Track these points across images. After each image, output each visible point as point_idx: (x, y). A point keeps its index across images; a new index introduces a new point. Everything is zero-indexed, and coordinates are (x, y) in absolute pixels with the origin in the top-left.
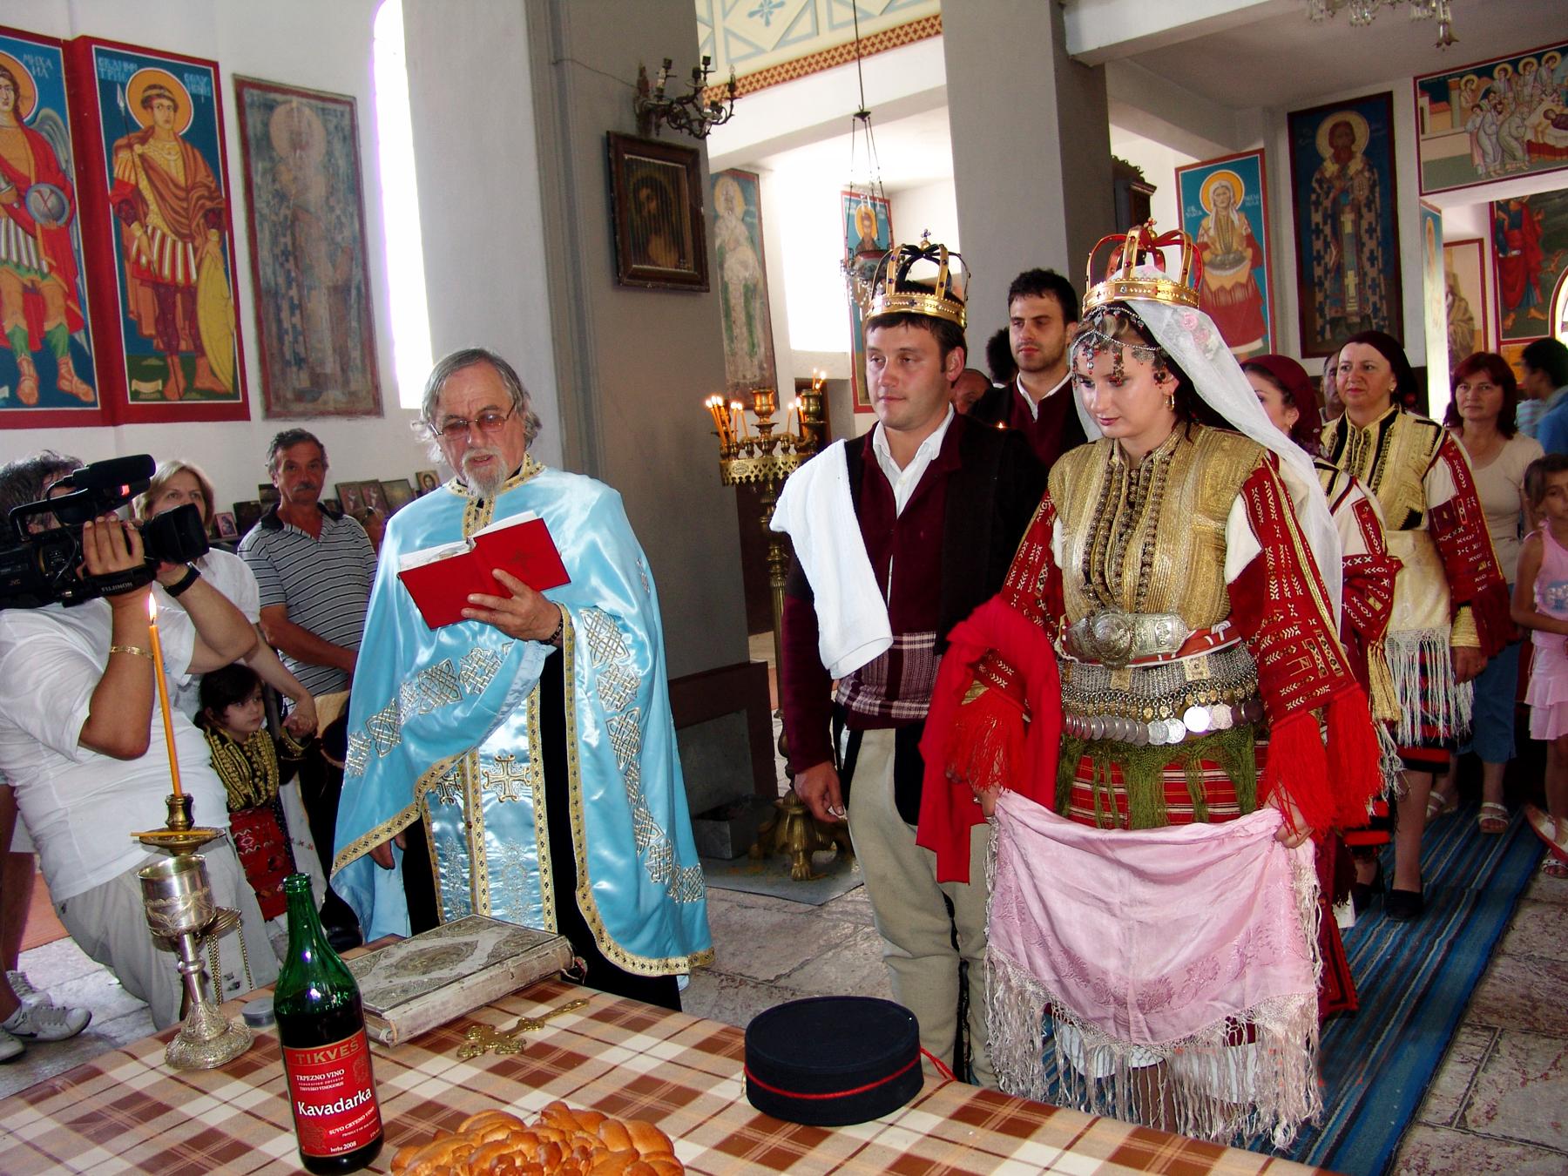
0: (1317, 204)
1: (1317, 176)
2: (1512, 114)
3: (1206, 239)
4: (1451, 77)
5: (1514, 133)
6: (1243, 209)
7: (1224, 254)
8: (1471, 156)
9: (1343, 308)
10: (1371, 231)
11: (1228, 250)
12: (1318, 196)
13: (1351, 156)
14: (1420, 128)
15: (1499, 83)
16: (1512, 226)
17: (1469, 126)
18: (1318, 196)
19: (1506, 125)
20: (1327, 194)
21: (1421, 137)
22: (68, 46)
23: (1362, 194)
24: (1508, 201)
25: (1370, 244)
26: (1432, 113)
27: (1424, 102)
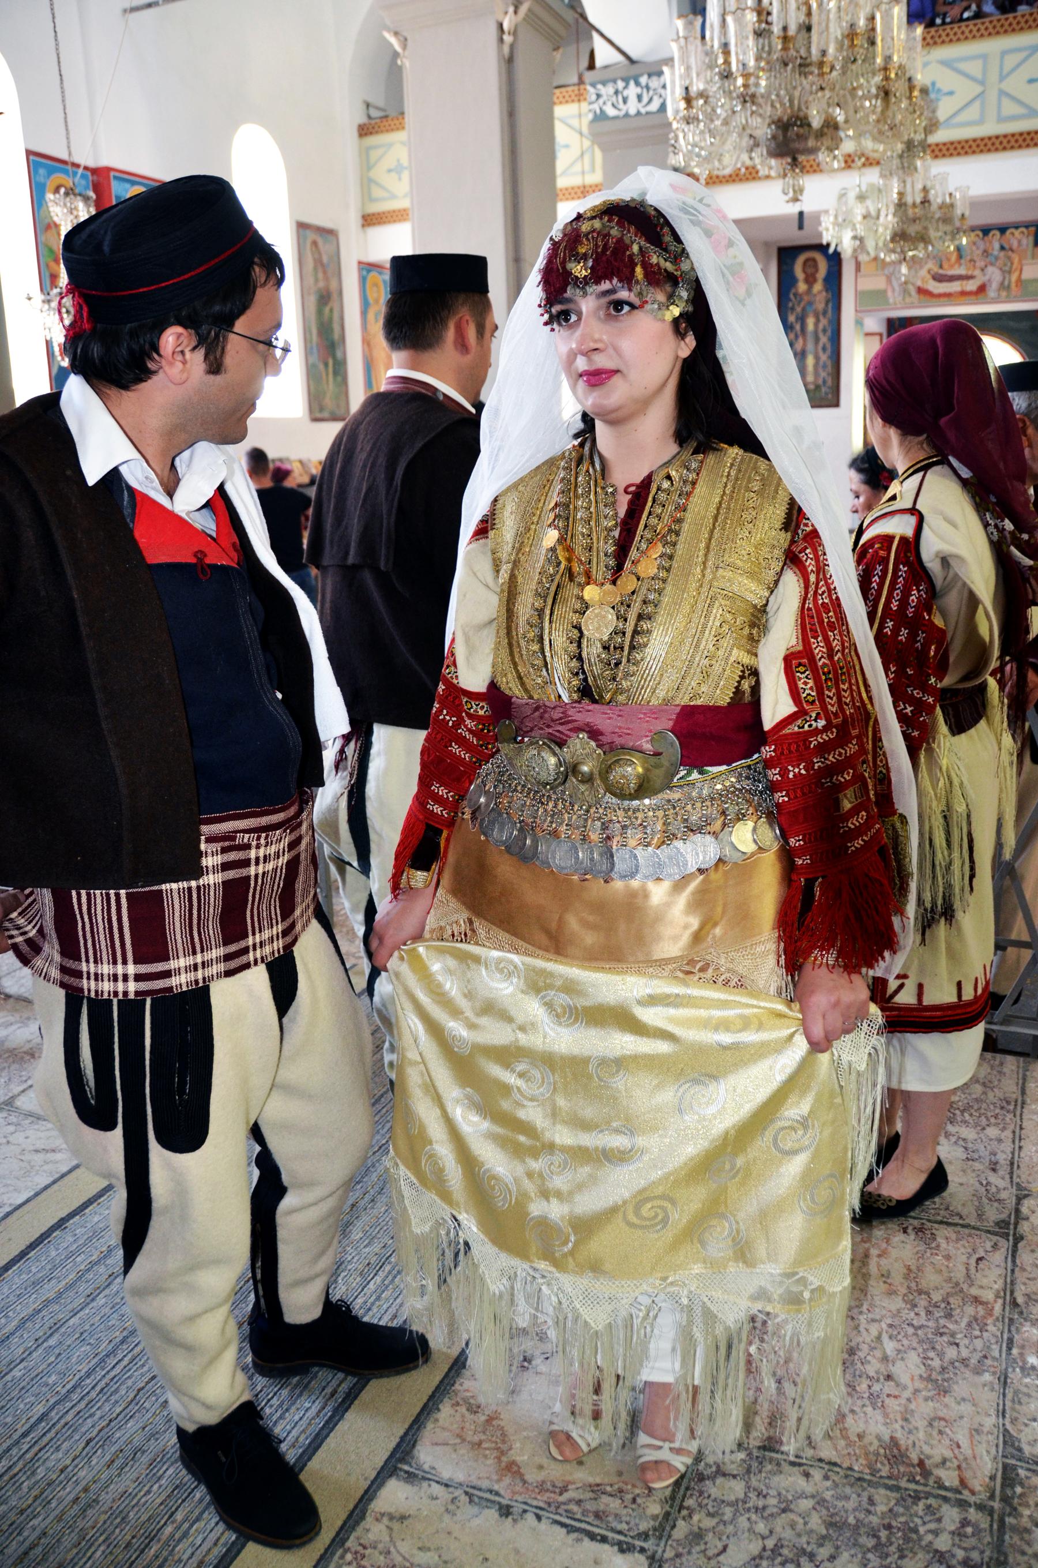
0: (793, 309)
1: (793, 291)
8: (885, 291)
10: (824, 331)
13: (815, 280)
20: (799, 303)
22: (95, 171)
23: (820, 306)
25: (824, 339)
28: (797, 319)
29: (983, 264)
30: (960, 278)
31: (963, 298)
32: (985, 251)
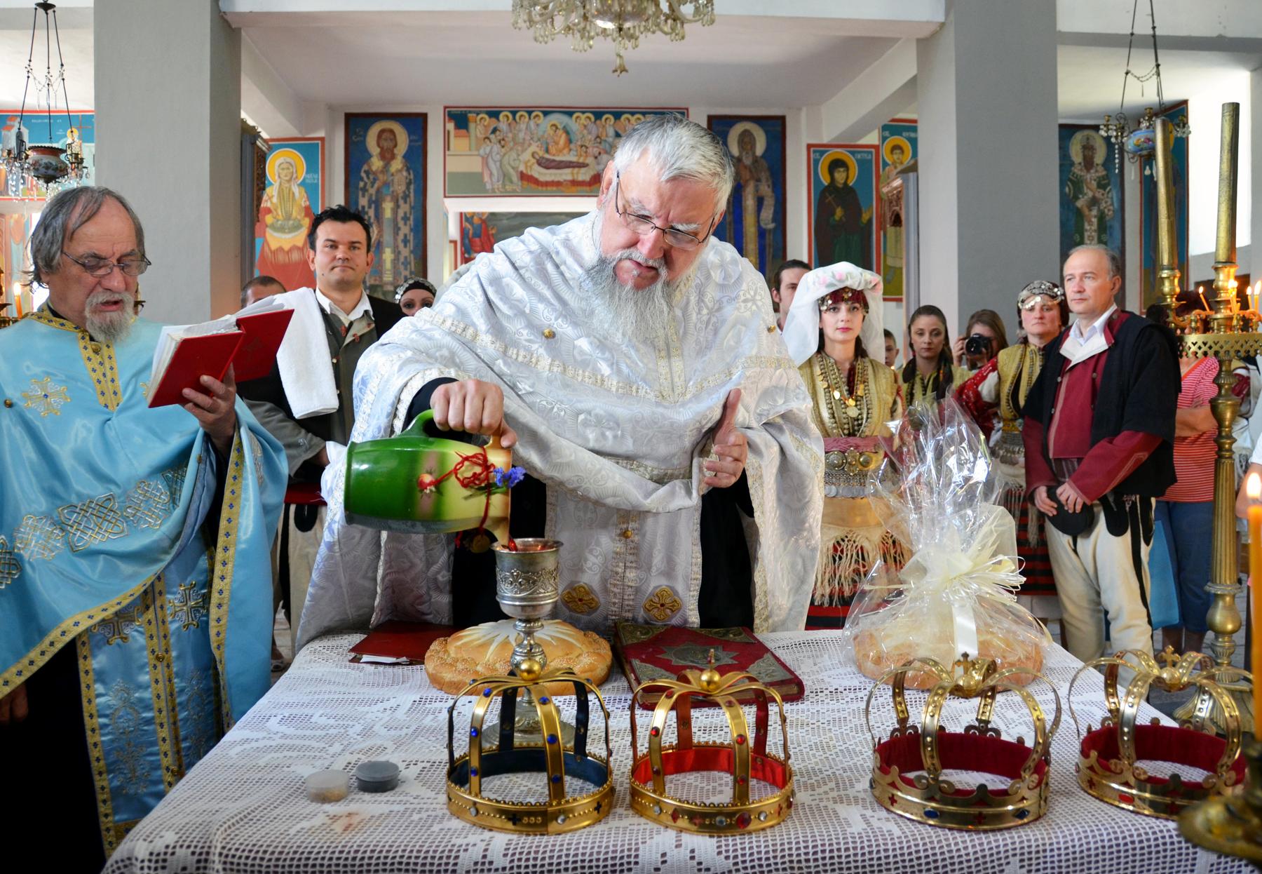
0: (364, 190)
1: (365, 167)
2: (511, 149)
3: (269, 205)
4: (470, 112)
5: (512, 163)
6: (303, 184)
7: (285, 219)
8: (481, 175)
9: (381, 278)
10: (405, 219)
11: (288, 217)
12: (366, 184)
13: (393, 157)
14: (447, 146)
15: (503, 124)
16: (475, 235)
17: (482, 152)
18: (366, 184)
19: (507, 156)
21: (447, 153)
23: (400, 188)
24: (473, 214)
25: (405, 230)
26: (455, 136)
27: (451, 126)
28: (370, 202)
29: (596, 151)
30: (569, 165)
31: (574, 189)
32: (598, 137)
